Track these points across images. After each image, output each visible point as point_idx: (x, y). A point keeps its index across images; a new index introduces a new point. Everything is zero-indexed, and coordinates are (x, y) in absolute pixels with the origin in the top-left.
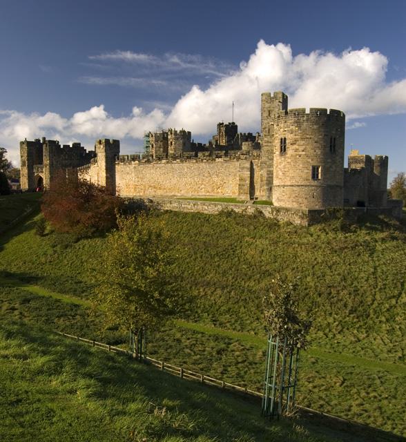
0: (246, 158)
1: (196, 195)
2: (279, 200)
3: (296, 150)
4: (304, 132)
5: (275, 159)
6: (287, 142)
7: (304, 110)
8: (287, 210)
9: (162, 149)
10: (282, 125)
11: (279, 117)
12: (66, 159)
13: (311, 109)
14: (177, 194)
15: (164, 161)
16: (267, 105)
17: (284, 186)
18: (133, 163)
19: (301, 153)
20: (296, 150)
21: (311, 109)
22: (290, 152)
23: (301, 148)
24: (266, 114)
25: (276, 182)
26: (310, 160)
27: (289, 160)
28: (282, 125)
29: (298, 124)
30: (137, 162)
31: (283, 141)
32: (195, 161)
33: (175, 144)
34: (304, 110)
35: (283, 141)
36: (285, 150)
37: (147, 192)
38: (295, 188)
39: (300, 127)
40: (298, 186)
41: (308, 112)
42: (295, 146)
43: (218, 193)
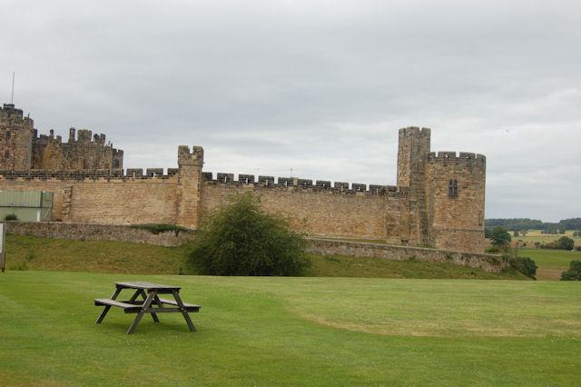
3: (468, 194)
7: (474, 155)
10: (452, 167)
16: (417, 140)
17: (455, 231)
18: (244, 186)
19: (472, 197)
20: (468, 194)
22: (462, 196)
23: (472, 193)
24: (415, 150)
27: (461, 204)
28: (452, 167)
29: (470, 167)
30: (251, 185)
33: (15, 137)
43: (357, 233)
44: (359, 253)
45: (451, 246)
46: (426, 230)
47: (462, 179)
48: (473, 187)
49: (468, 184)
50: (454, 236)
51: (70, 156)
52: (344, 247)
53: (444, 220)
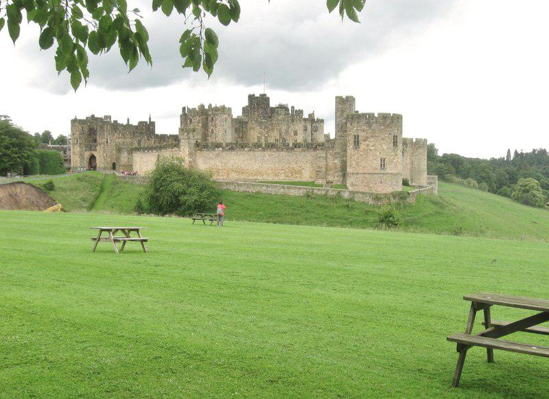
0: (322, 149)
1: (276, 179)
2: (352, 185)
3: (368, 145)
4: (374, 132)
5: (349, 151)
6: (360, 138)
7: (373, 114)
8: (363, 193)
9: (200, 125)
11: (352, 118)
12: (119, 138)
13: (379, 114)
14: (259, 177)
15: (246, 149)
18: (216, 149)
19: (371, 148)
21: (379, 114)
22: (362, 146)
25: (349, 170)
26: (378, 153)
30: (221, 149)
31: (356, 137)
32: (275, 150)
34: (373, 114)
35: (356, 137)
36: (358, 144)
37: (231, 176)
38: (366, 176)
39: (370, 128)
40: (369, 174)
41: (376, 115)
42: (367, 143)
44: (272, 190)
45: (355, 185)
46: (344, 174)
47: (362, 134)
48: (372, 139)
49: (367, 138)
50: (357, 178)
51: (266, 127)
52: (264, 188)
53: (351, 166)
